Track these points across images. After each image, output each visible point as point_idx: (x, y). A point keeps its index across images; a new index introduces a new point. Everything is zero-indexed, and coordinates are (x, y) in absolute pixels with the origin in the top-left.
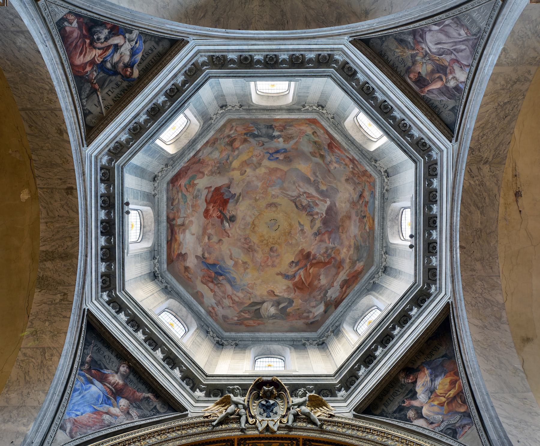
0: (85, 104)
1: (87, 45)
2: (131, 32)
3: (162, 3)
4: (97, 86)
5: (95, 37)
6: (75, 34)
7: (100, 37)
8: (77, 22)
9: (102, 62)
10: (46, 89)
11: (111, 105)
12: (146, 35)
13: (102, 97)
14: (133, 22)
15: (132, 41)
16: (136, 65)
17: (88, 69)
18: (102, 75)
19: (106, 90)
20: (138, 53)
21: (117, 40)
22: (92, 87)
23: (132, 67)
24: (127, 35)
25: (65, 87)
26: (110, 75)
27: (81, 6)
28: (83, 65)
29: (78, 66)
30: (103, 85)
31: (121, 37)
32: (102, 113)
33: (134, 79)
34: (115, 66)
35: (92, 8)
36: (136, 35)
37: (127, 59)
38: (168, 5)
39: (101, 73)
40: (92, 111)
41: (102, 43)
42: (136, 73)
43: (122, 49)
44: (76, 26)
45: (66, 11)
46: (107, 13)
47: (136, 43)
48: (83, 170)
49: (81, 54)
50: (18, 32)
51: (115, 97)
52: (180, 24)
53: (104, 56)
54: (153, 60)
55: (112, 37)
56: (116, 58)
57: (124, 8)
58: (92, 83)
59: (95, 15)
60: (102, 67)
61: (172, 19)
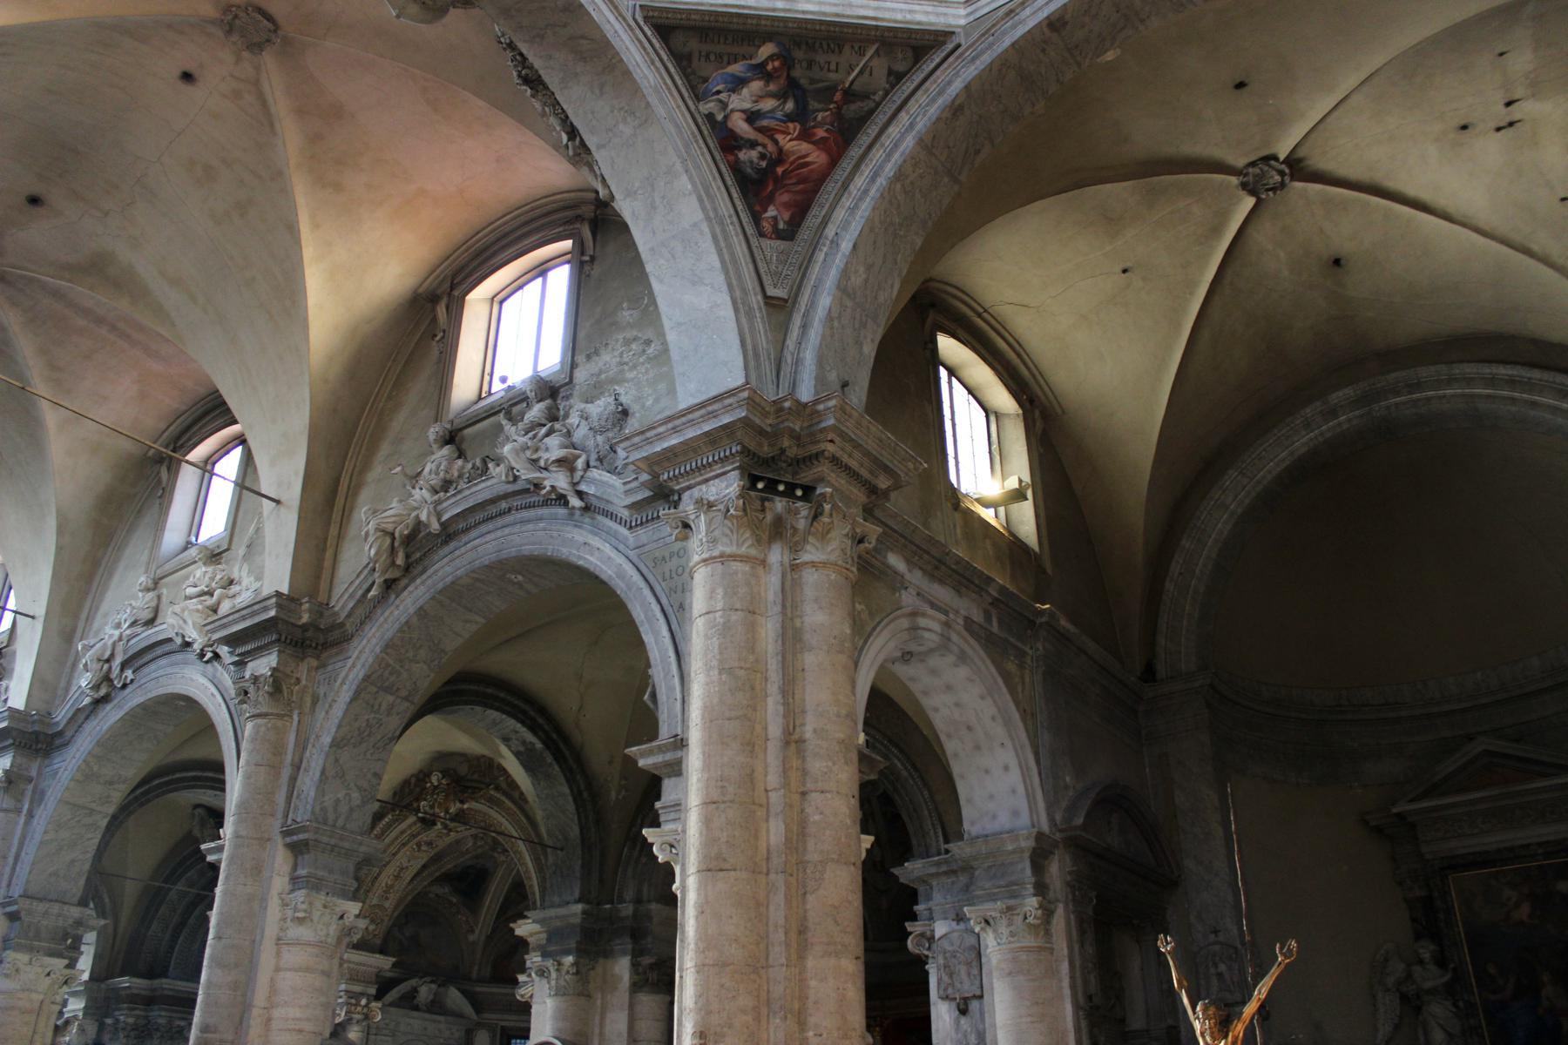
0: (881, 93)
1: (786, 166)
2: (710, 117)
3: (629, 119)
4: (838, 96)
5: (764, 164)
6: (785, 197)
7: (758, 158)
8: (766, 211)
9: (792, 121)
10: (903, 185)
11: (852, 47)
12: (693, 88)
13: (849, 74)
14: (695, 137)
15: (720, 101)
16: (754, 62)
17: (821, 133)
18: (814, 105)
19: (833, 76)
20: (733, 75)
21: (740, 125)
22: (844, 104)
23: (763, 65)
24: (720, 117)
25: (877, 154)
26: (804, 91)
27: (741, 237)
28: (821, 146)
29: (827, 150)
30: (827, 89)
31: (730, 125)
32: (877, 51)
33: (779, 44)
34: (782, 96)
35: (730, 216)
36: (706, 103)
37: (756, 86)
38: (621, 109)
39: (811, 107)
40: (885, 72)
41: (764, 146)
42: (767, 50)
43: (747, 105)
44: (771, 208)
45: (766, 243)
46: (719, 188)
47: (718, 92)
48: (1002, 19)
49: (807, 164)
50: (849, 295)
51: (833, 52)
52: (631, 68)
53: (781, 126)
54: (722, 40)
55: (742, 138)
56: (768, 104)
57: (691, 178)
58: (839, 108)
59: (735, 195)
60: (801, 115)
61: (636, 90)
